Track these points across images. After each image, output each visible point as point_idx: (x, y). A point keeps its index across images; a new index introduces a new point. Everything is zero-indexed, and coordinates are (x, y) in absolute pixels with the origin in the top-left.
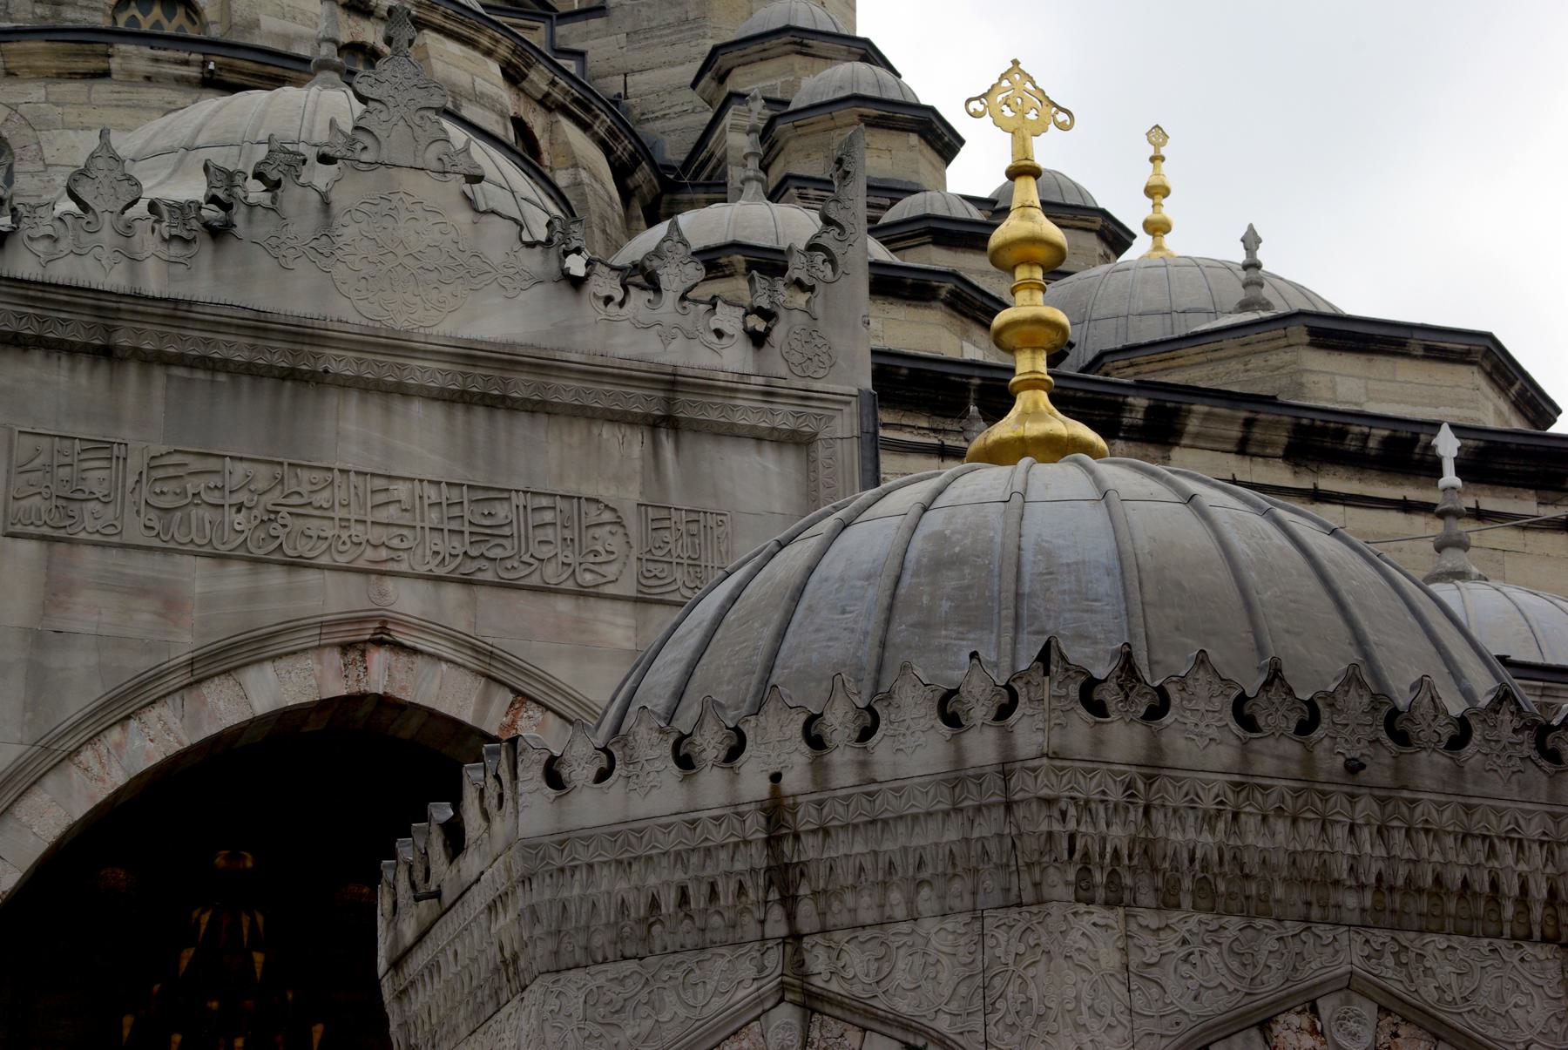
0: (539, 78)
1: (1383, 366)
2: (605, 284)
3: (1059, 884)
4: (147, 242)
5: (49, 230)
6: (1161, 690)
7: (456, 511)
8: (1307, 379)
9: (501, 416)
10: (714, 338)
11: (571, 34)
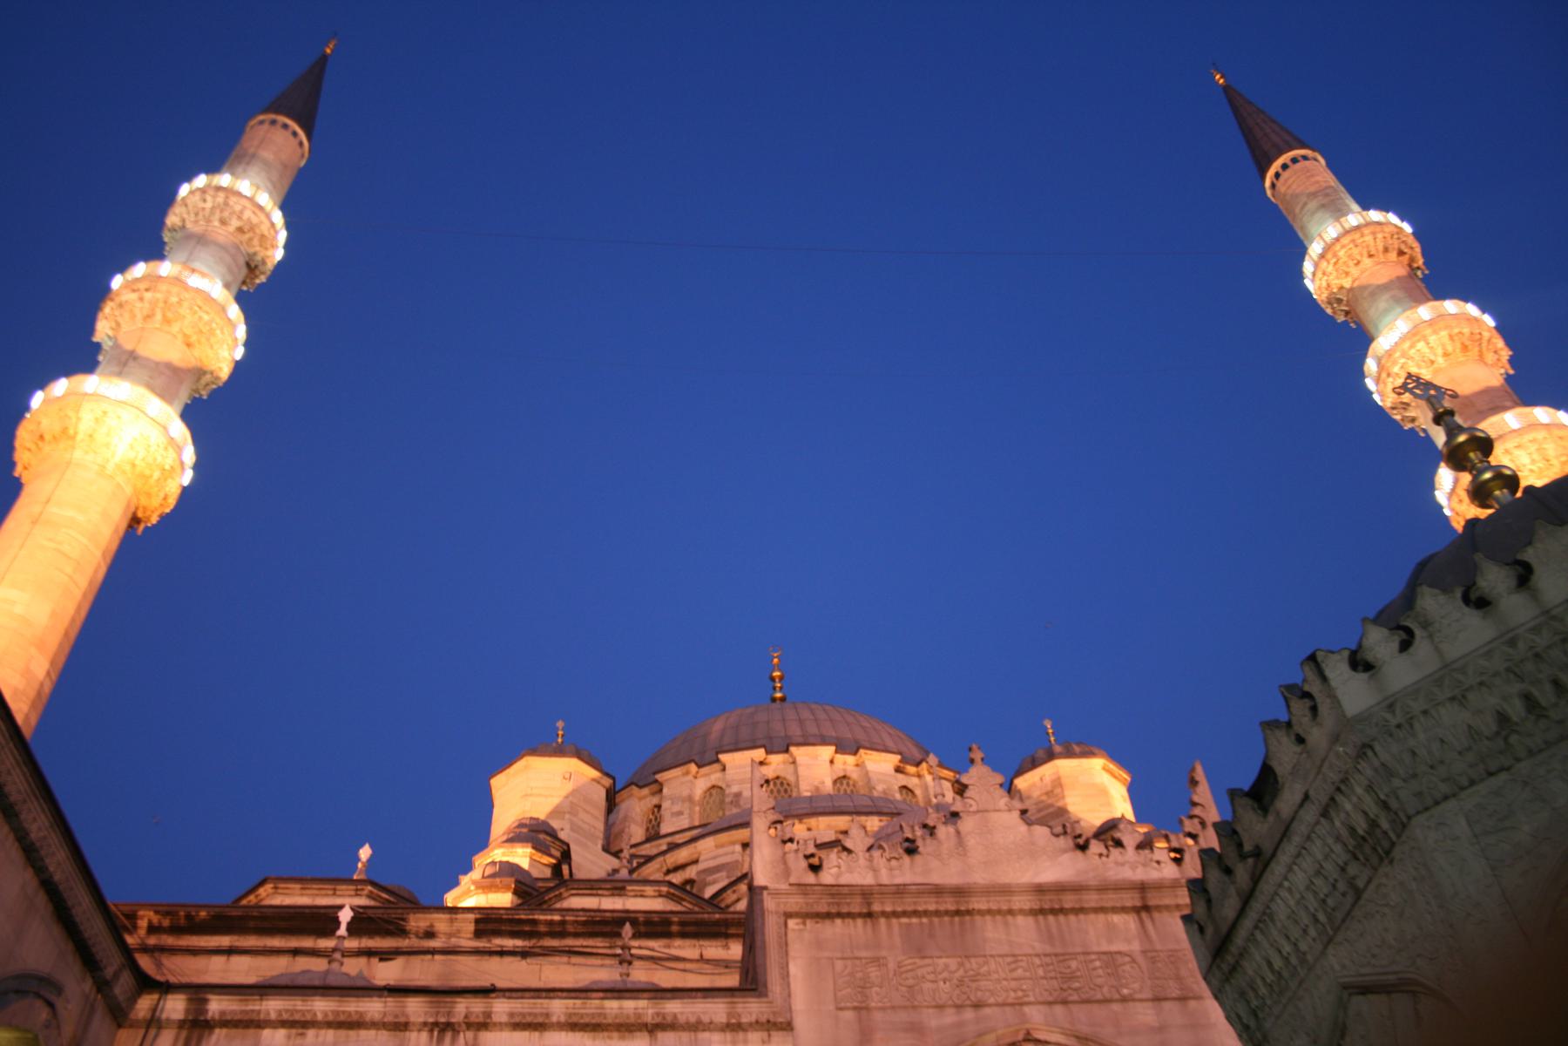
5: (835, 864)
7: (1051, 967)
10: (1155, 865)
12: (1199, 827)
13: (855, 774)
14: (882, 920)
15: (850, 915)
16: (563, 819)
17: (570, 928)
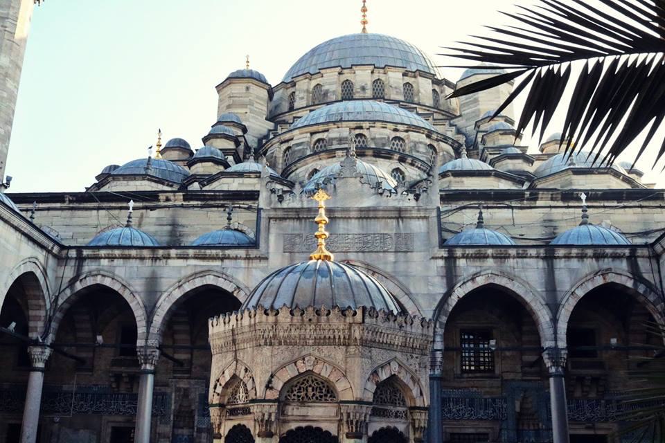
0: (434, 136)
1: (589, 177)
3: (262, 342)
4: (304, 196)
6: (278, 310)
9: (369, 220)
11: (454, 121)
13: (383, 77)
14: (303, 221)
15: (293, 219)
16: (246, 107)
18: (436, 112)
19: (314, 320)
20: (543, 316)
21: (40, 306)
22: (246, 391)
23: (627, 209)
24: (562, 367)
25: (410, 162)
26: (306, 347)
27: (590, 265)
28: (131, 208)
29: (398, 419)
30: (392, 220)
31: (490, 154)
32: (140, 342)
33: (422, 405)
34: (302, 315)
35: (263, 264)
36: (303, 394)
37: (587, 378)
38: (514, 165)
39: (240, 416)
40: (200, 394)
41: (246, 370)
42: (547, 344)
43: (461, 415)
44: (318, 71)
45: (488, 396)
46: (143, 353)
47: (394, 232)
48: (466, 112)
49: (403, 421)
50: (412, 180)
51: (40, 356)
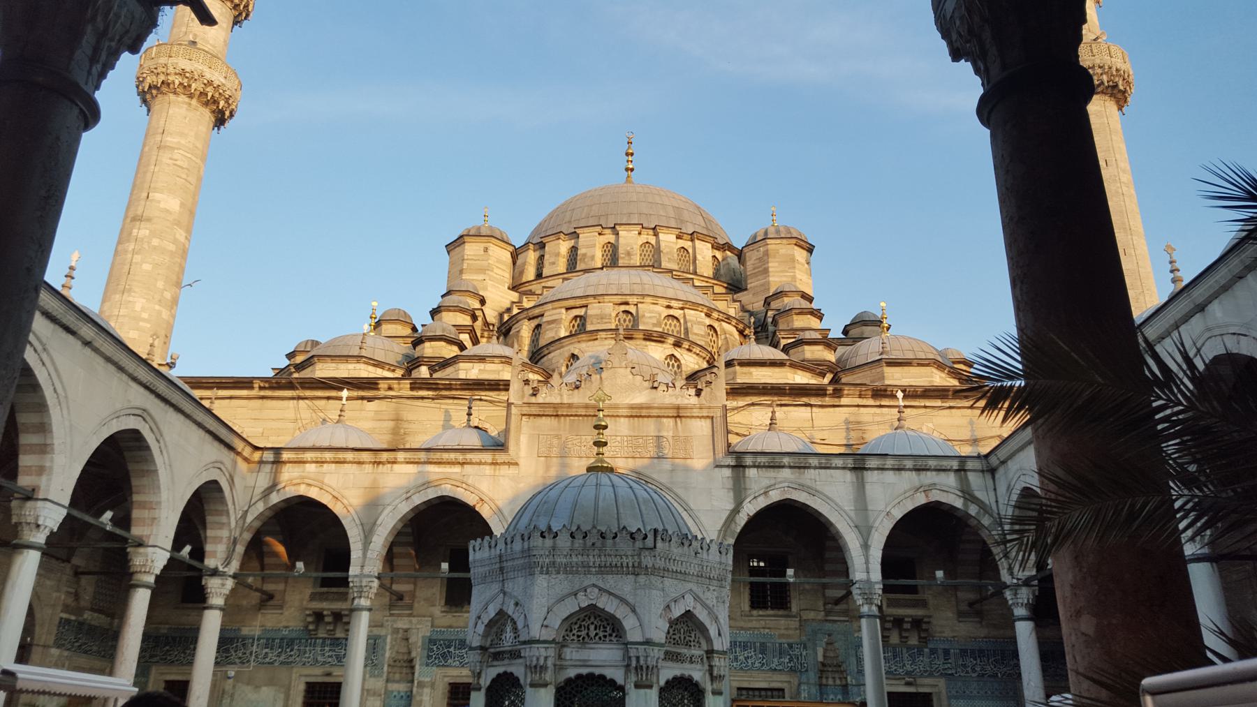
0: (715, 315)
2: (663, 387)
8: (886, 374)
9: (640, 419)
12: (714, 378)
17: (454, 387)
18: (716, 284)
19: (598, 544)
20: (852, 540)
21: (224, 524)
22: (515, 629)
23: (953, 411)
24: (877, 605)
25: (687, 347)
26: (589, 576)
27: (911, 478)
28: (344, 399)
29: (693, 666)
30: (669, 419)
31: (783, 338)
32: (354, 570)
33: (720, 649)
34: (584, 537)
35: (512, 471)
36: (583, 633)
37: (906, 619)
38: (813, 352)
39: (506, 662)
40: (423, 637)
41: (517, 604)
42: (858, 574)
43: (750, 664)
44: (573, 230)
45: (784, 641)
46: (358, 585)
47: (671, 434)
48: (753, 285)
49: (699, 666)
50: (689, 369)
51: (218, 590)
